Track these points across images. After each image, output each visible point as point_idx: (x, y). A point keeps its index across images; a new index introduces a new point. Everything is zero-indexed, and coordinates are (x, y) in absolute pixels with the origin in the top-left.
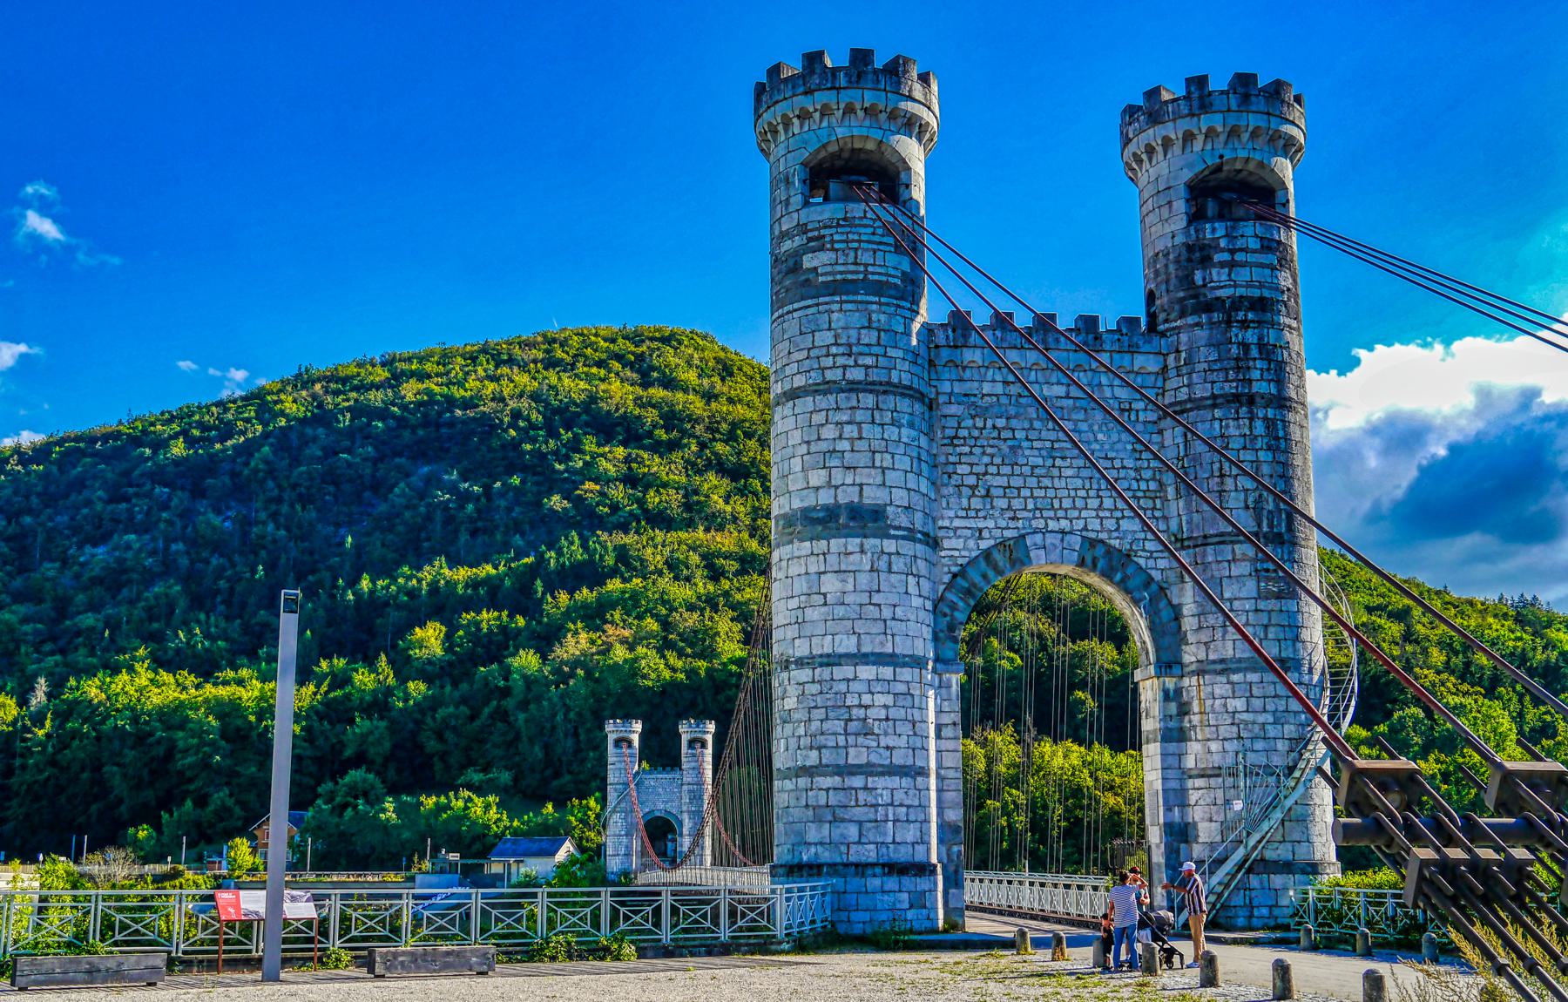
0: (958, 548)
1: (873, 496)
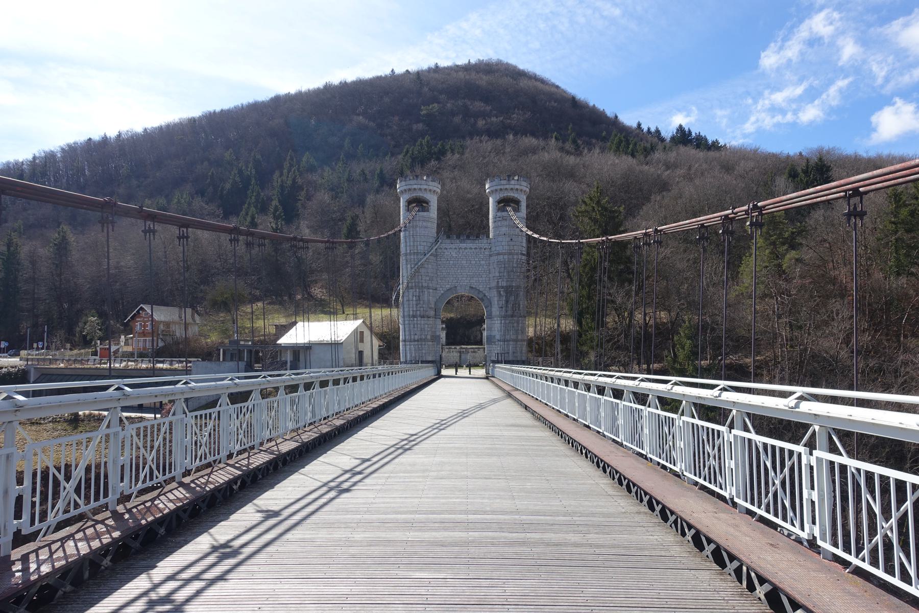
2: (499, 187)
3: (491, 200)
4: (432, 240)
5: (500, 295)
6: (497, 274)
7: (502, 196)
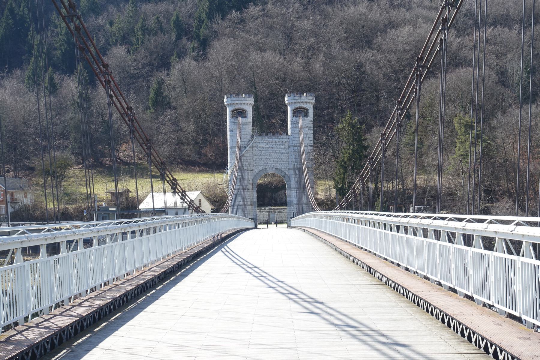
2: (294, 101)
3: (289, 109)
4: (249, 137)
5: (296, 174)
6: (294, 160)
7: (296, 107)
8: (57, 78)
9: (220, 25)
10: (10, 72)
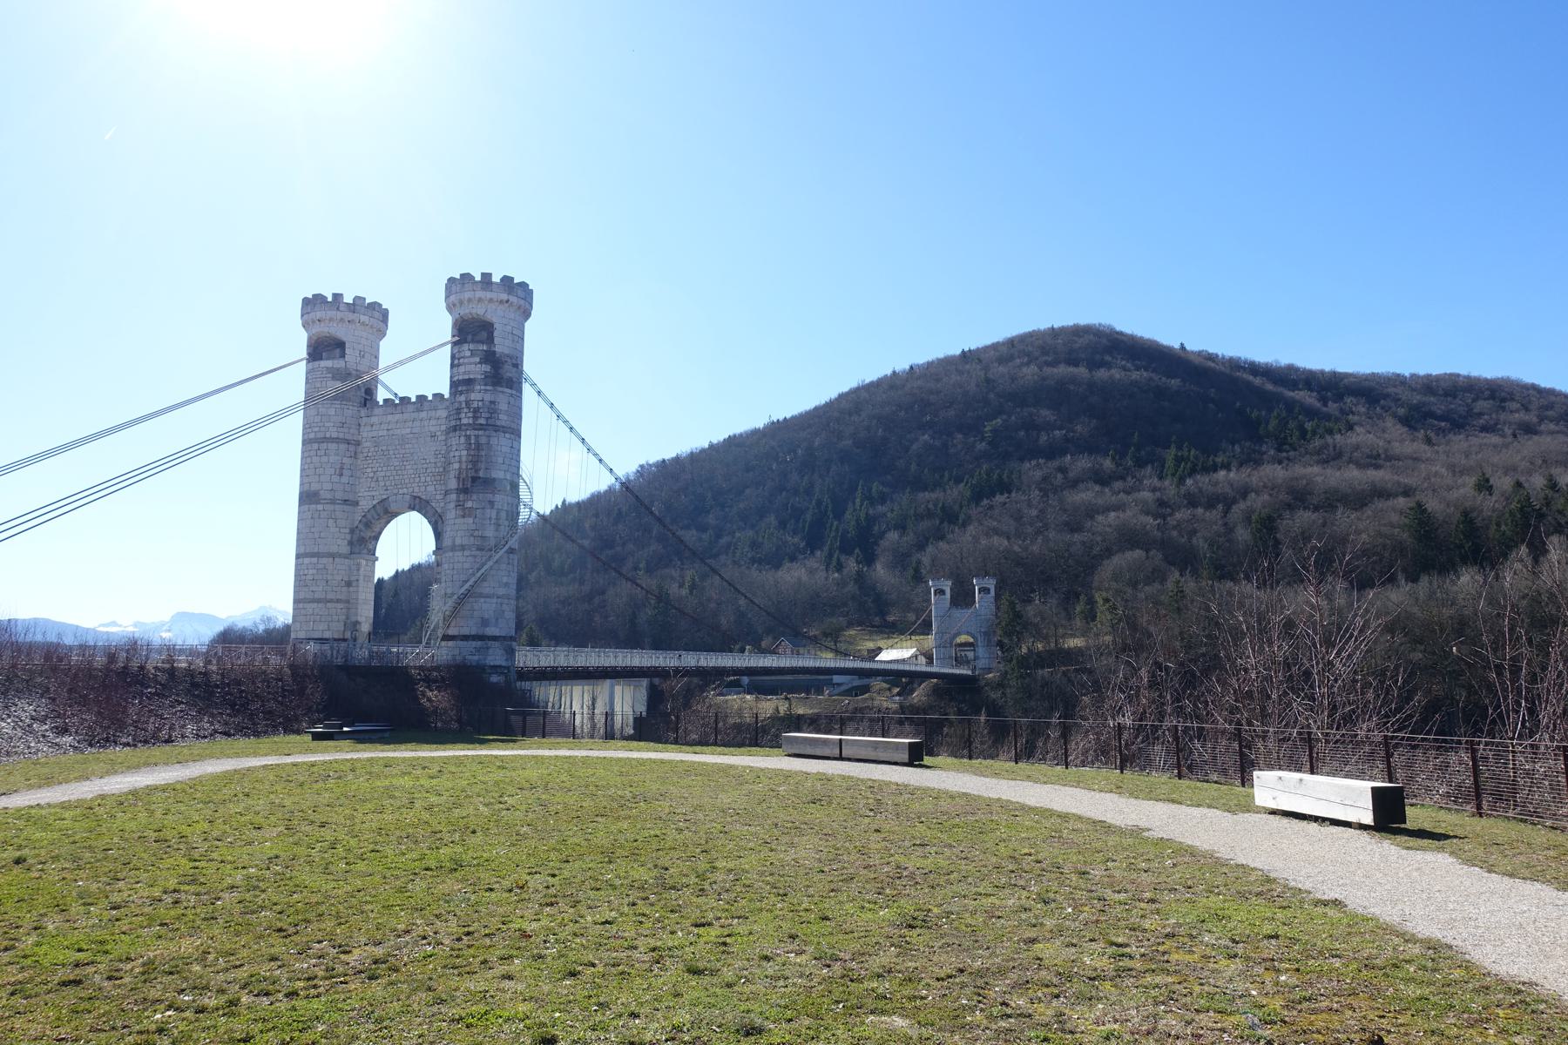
0: (366, 504)
1: (315, 487)
8: (843, 558)
9: (974, 511)
10: (812, 552)
